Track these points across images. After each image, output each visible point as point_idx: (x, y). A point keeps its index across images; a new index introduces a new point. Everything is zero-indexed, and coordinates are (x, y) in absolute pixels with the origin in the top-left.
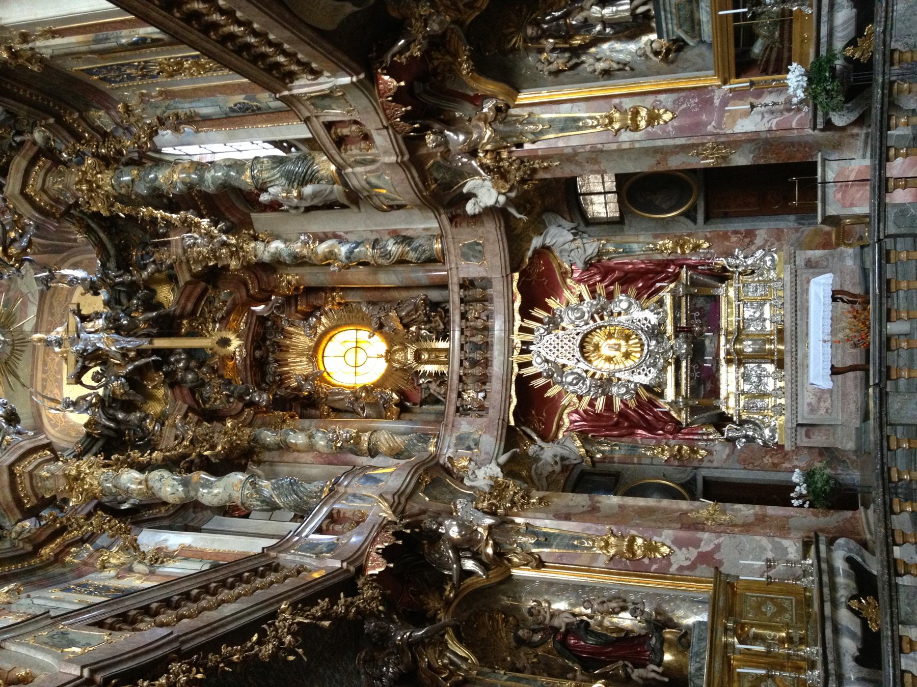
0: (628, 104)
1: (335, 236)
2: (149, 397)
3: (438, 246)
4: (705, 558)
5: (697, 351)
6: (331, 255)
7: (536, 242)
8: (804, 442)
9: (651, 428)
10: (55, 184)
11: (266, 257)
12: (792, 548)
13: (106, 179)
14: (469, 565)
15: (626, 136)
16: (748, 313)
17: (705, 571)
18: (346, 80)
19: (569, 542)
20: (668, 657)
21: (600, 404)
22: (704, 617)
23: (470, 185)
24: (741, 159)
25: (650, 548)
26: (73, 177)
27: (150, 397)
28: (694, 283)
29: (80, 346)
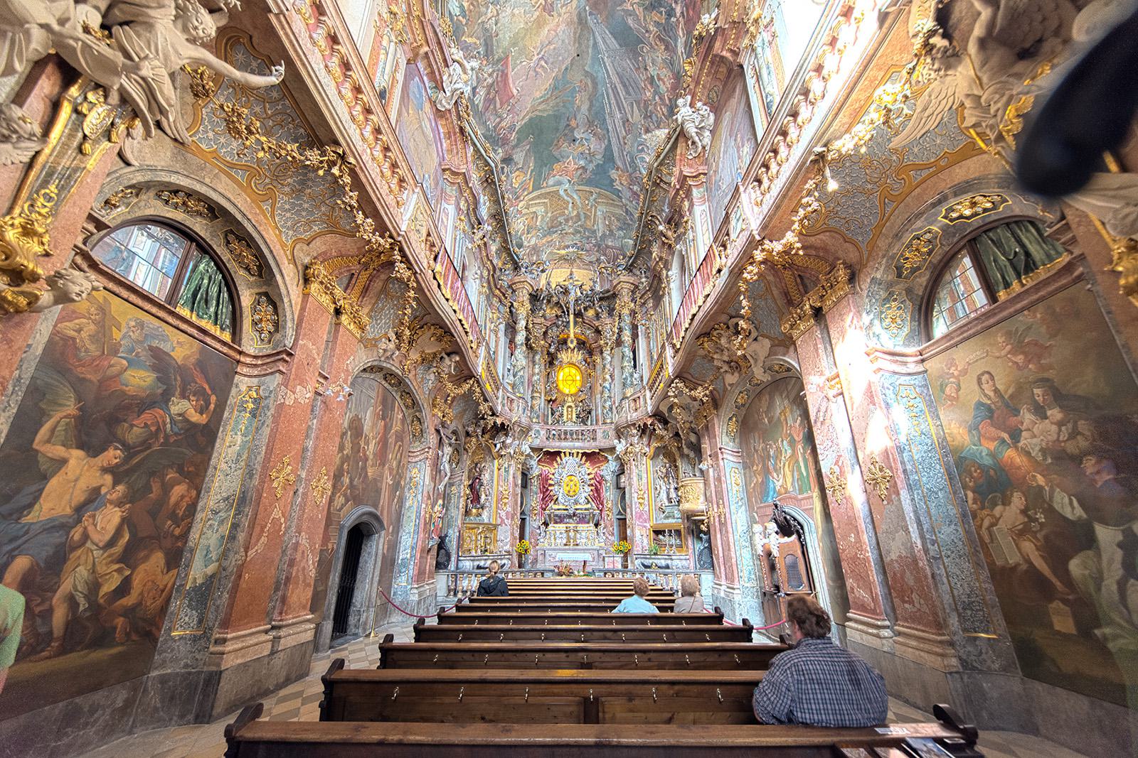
0: (646, 496)
1: (613, 380)
2: (552, 308)
3: (608, 421)
4: (503, 520)
5: (570, 517)
6: (605, 380)
7: (610, 457)
8: (539, 553)
9: (543, 499)
10: (625, 292)
11: (604, 355)
12: (507, 548)
13: (626, 312)
14: (498, 446)
15: (636, 495)
16: (583, 534)
17: (499, 521)
18: (649, 409)
19: (506, 480)
20: (474, 511)
21: (551, 482)
22: (486, 521)
23: (623, 441)
24: (629, 531)
25: (505, 504)
26: (627, 299)
27: (552, 308)
28: (594, 515)
29: (571, 287)
